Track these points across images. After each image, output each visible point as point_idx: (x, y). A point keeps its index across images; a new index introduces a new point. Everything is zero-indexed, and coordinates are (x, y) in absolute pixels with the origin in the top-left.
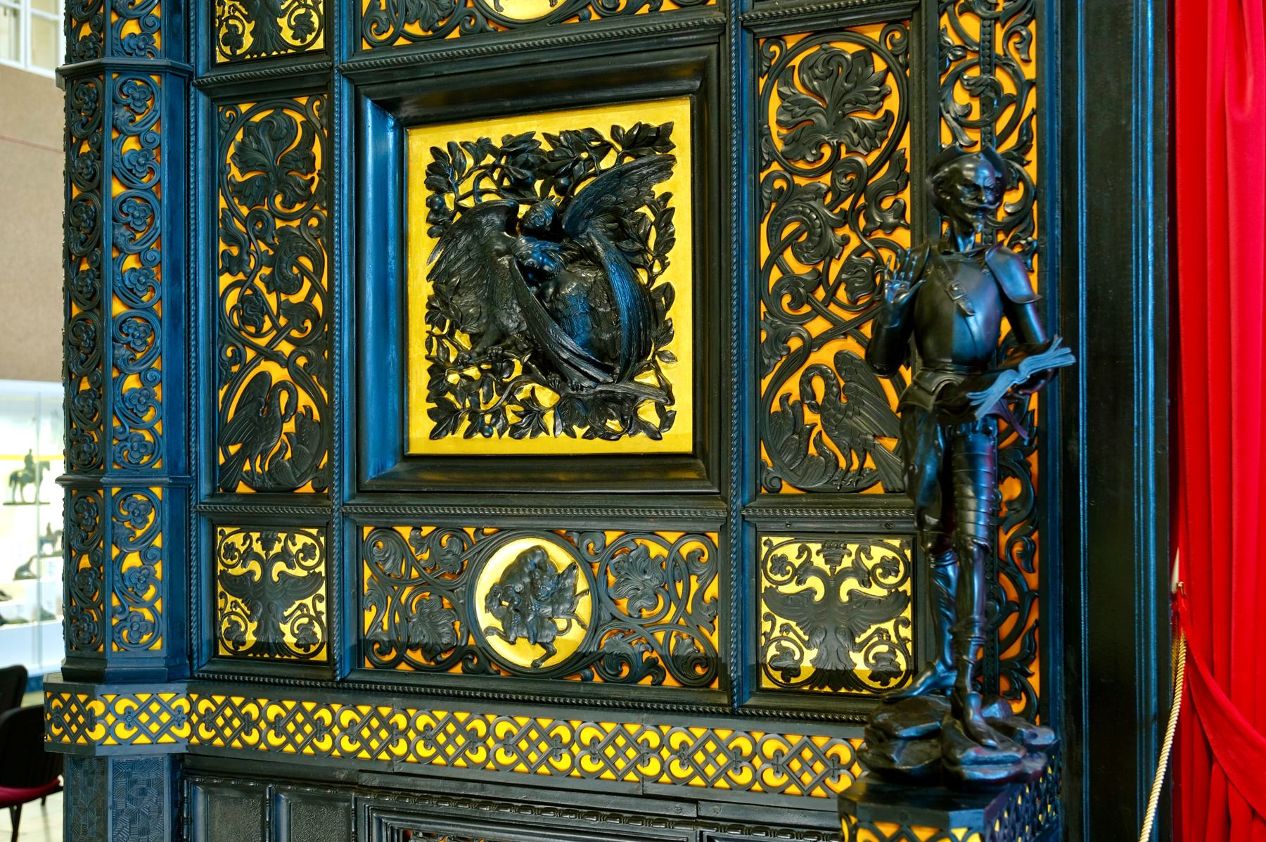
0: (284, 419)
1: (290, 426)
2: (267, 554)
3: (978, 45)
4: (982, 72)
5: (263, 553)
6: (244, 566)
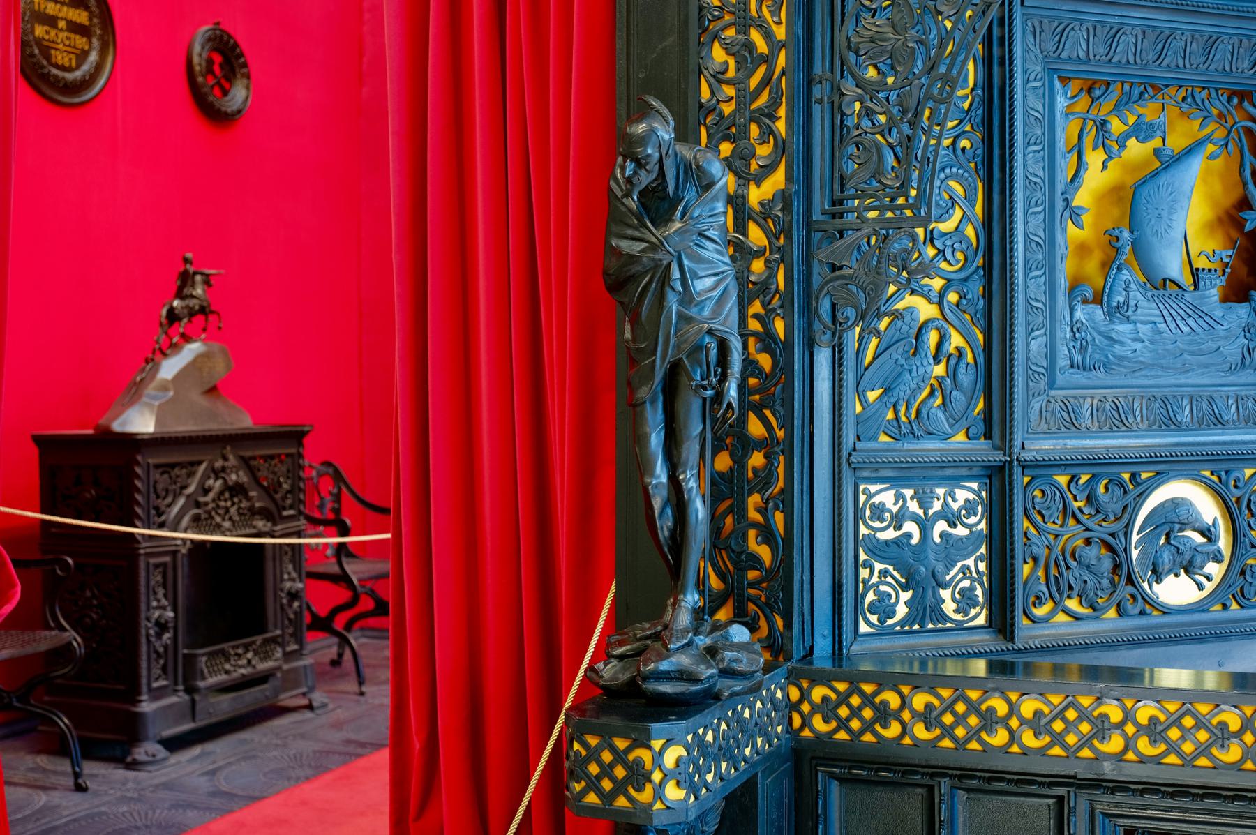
2: (925, 514)
3: (733, 6)
4: (738, 32)
5: (921, 512)
6: (898, 527)
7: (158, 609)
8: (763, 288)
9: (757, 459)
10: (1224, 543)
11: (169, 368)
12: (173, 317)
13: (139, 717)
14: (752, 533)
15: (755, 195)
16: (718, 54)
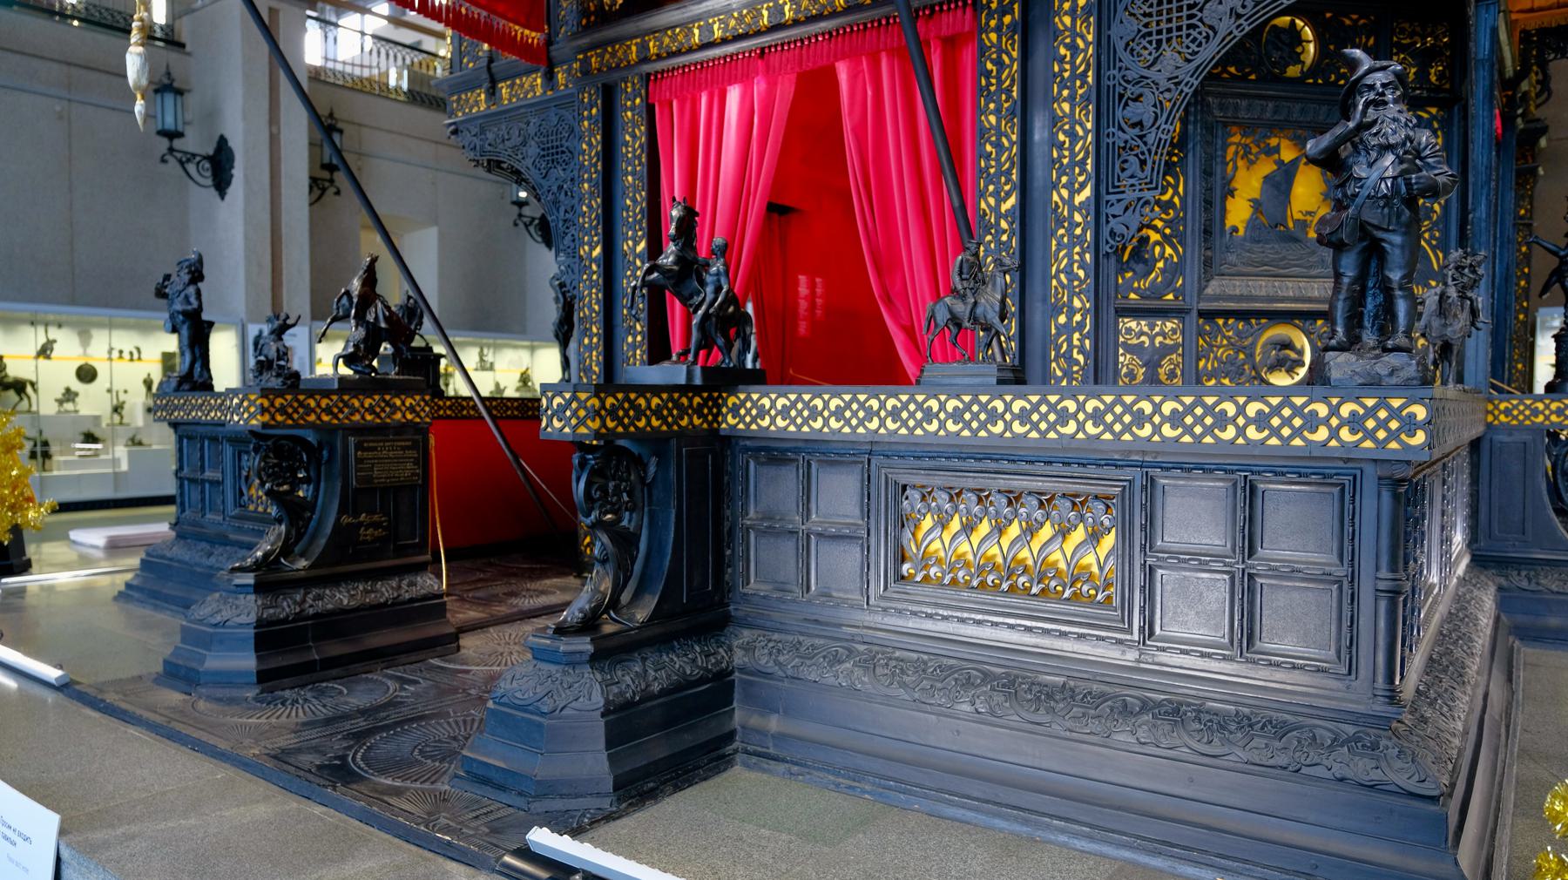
0: (1157, 261)
1: (1160, 265)
10: (1307, 359)
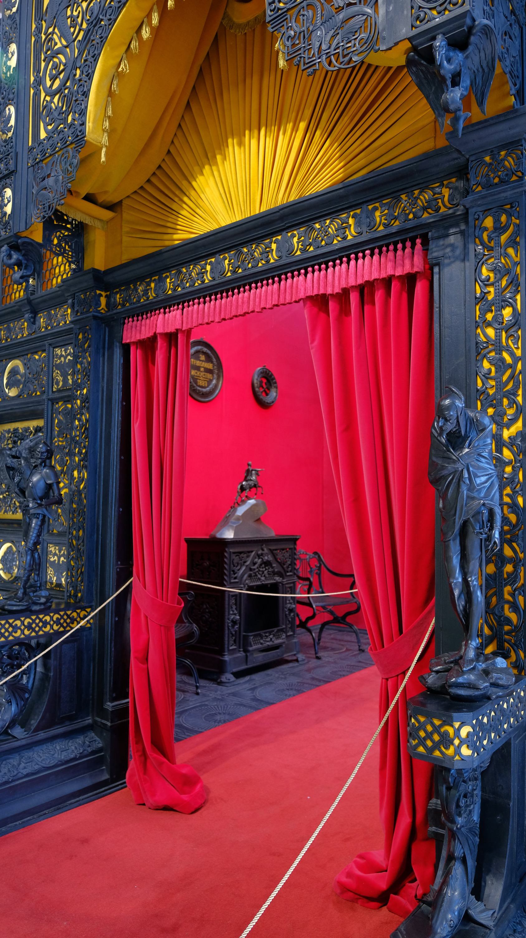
7: (233, 615)
8: (512, 480)
9: (509, 568)
11: (241, 511)
12: (243, 489)
13: (225, 661)
14: (506, 607)
15: (506, 434)
16: (486, 364)
